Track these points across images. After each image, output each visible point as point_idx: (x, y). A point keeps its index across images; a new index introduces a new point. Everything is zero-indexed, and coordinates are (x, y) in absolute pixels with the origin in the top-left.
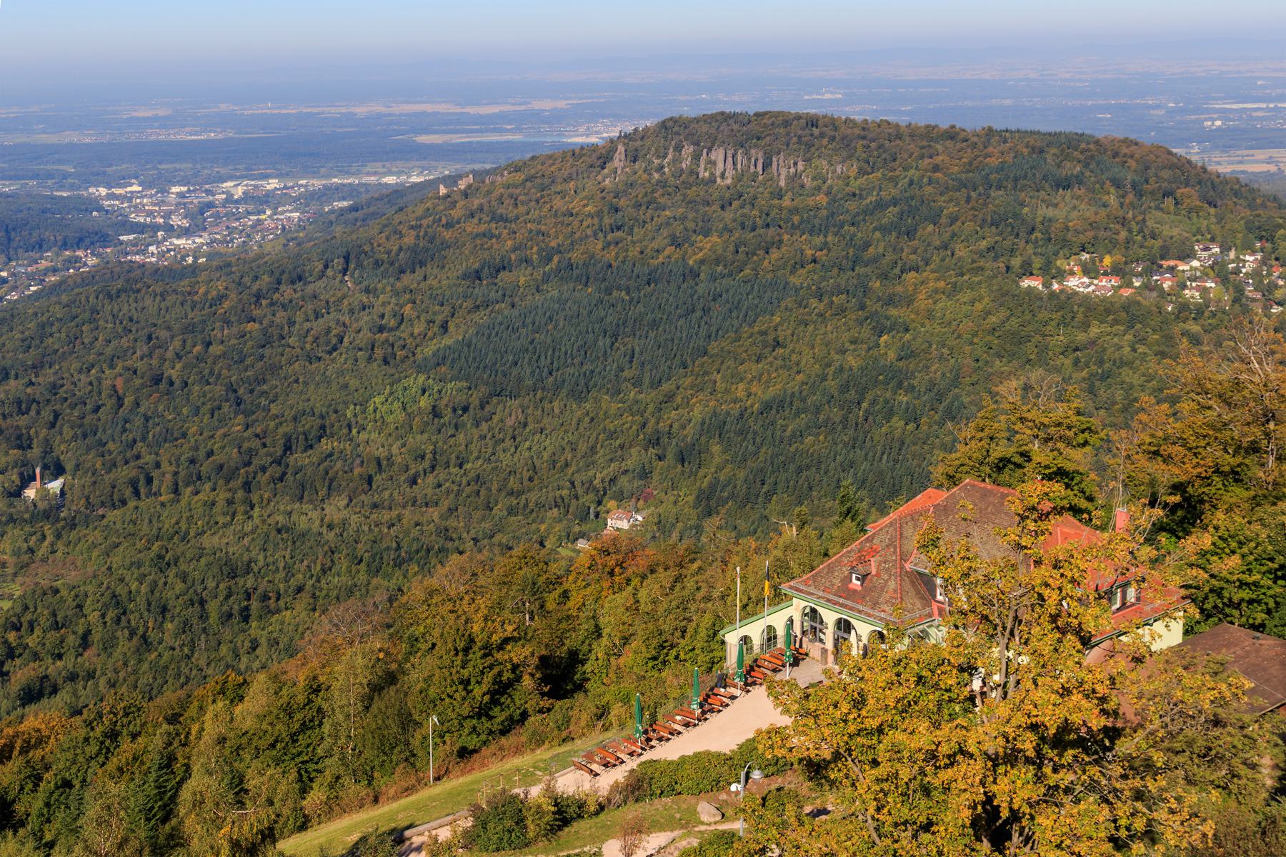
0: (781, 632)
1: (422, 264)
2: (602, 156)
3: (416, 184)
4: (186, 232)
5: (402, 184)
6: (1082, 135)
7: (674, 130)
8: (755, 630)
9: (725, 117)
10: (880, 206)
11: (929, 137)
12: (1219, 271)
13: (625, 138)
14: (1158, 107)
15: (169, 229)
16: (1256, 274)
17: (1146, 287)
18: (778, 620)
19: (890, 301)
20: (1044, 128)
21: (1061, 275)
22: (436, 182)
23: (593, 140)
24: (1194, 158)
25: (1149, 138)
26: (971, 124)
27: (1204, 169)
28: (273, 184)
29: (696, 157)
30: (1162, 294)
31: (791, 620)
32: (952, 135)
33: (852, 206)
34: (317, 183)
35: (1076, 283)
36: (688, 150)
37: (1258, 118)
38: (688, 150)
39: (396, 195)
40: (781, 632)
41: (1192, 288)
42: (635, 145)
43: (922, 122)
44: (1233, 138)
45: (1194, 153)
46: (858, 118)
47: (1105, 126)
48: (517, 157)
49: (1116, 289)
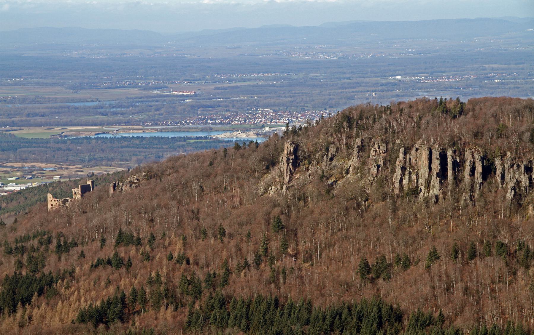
1: (27, 301)
3: (14, 195)
22: (43, 190)
29: (390, 160)
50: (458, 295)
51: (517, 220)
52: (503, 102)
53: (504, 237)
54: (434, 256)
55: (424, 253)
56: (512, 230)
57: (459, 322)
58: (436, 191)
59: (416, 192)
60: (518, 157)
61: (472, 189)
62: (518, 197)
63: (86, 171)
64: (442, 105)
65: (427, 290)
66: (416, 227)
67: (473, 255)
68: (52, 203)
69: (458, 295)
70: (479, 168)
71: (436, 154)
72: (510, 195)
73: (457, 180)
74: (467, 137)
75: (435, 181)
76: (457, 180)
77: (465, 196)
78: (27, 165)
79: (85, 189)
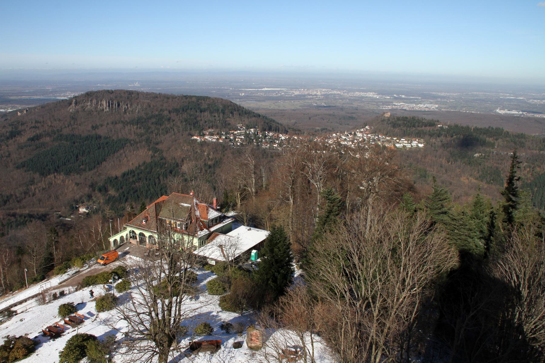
0: (125, 237)
1: (15, 136)
2: (69, 102)
3: (10, 112)
5: (6, 112)
6: (207, 97)
7: (89, 95)
8: (117, 237)
13: (75, 97)
14: (227, 89)
17: (226, 138)
19: (157, 144)
21: (204, 135)
22: (16, 111)
23: (66, 98)
24: (237, 103)
25: (226, 98)
27: (240, 107)
29: (97, 103)
30: (231, 140)
31: (127, 234)
36: (94, 101)
37: (254, 93)
38: (94, 101)
40: (125, 237)
41: (238, 138)
44: (247, 98)
45: (237, 102)
46: (145, 91)
47: (214, 94)
49: (218, 139)
50: (113, 132)
51: (125, 116)
52: (121, 91)
53: (122, 119)
54: (108, 124)
55: (105, 123)
56: (124, 118)
57: (113, 138)
58: (108, 110)
59: (103, 110)
60: (125, 102)
61: (115, 109)
62: (125, 111)
63: (27, 107)
64: (108, 91)
65: (106, 131)
66: (104, 118)
67: (116, 123)
68: (19, 114)
69: (113, 132)
70: (117, 105)
71: (107, 102)
72: (123, 110)
73: (112, 107)
74: (114, 98)
75: (107, 108)
76: (112, 107)
77: (114, 111)
78: (13, 105)
79: (27, 111)
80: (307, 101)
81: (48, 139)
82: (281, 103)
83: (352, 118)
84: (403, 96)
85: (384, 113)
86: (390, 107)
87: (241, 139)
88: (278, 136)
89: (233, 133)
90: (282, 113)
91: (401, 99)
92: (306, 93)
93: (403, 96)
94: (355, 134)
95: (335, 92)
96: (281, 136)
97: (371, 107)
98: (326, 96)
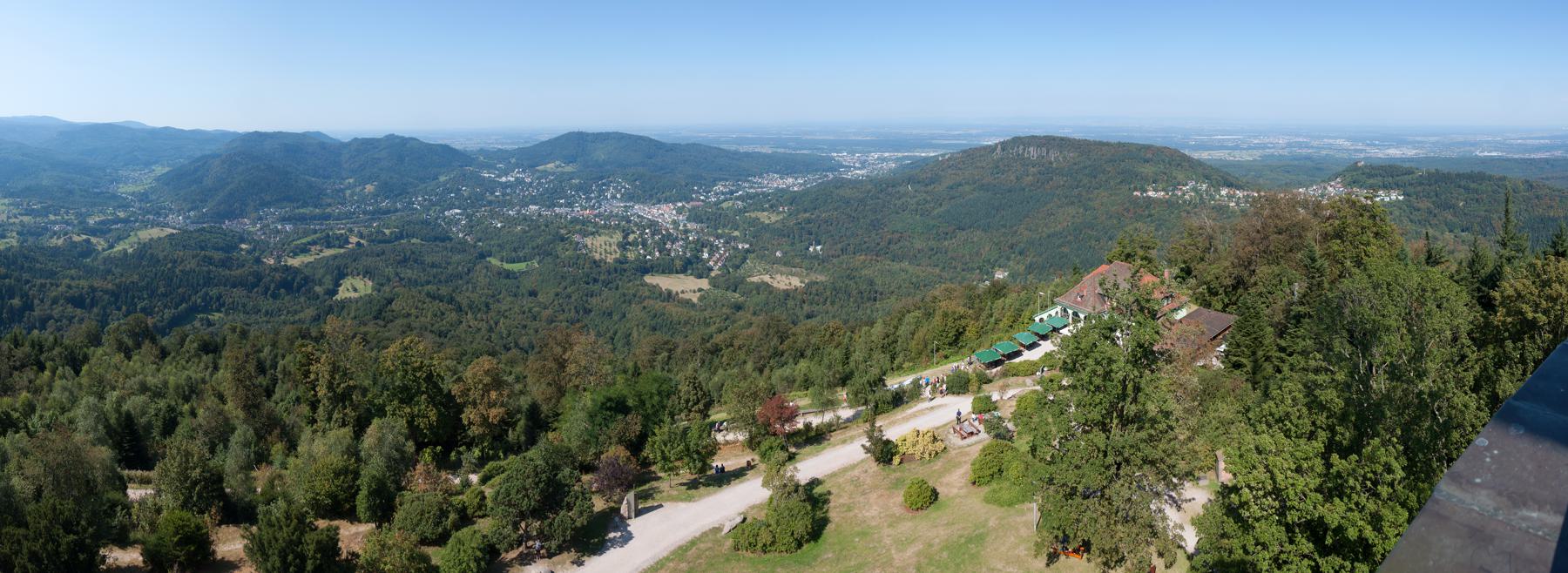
2: (992, 149)
4: (859, 169)
9: (1034, 137)
10: (1085, 168)
11: (1101, 144)
12: (1194, 189)
15: (854, 167)
16: (1206, 191)
18: (1053, 312)
20: (1141, 143)
23: (990, 143)
26: (1113, 141)
28: (886, 154)
29: (1024, 149)
32: (1108, 144)
33: (1076, 167)
34: (900, 155)
35: (1151, 194)
39: (925, 159)
42: (1004, 145)
43: (1098, 140)
46: (1077, 138)
47: (1159, 143)
48: (964, 148)
80: (1268, 150)
81: (967, 188)
82: (1237, 153)
83: (1319, 169)
84: (1377, 142)
85: (1357, 163)
86: (1362, 156)
87: (1191, 196)
88: (1234, 193)
89: (1181, 189)
90: (1238, 165)
91: (1375, 145)
92: (1267, 141)
93: (1377, 142)
94: (1325, 188)
95: (1301, 140)
96: (1238, 192)
97: (1345, 156)
98: (1289, 145)
